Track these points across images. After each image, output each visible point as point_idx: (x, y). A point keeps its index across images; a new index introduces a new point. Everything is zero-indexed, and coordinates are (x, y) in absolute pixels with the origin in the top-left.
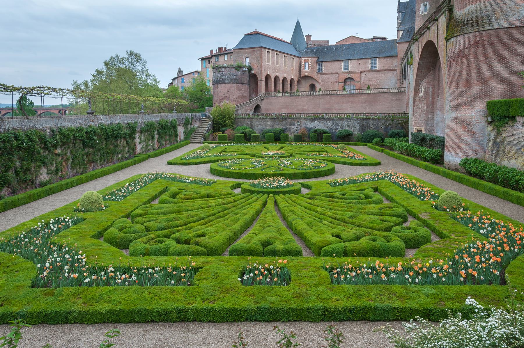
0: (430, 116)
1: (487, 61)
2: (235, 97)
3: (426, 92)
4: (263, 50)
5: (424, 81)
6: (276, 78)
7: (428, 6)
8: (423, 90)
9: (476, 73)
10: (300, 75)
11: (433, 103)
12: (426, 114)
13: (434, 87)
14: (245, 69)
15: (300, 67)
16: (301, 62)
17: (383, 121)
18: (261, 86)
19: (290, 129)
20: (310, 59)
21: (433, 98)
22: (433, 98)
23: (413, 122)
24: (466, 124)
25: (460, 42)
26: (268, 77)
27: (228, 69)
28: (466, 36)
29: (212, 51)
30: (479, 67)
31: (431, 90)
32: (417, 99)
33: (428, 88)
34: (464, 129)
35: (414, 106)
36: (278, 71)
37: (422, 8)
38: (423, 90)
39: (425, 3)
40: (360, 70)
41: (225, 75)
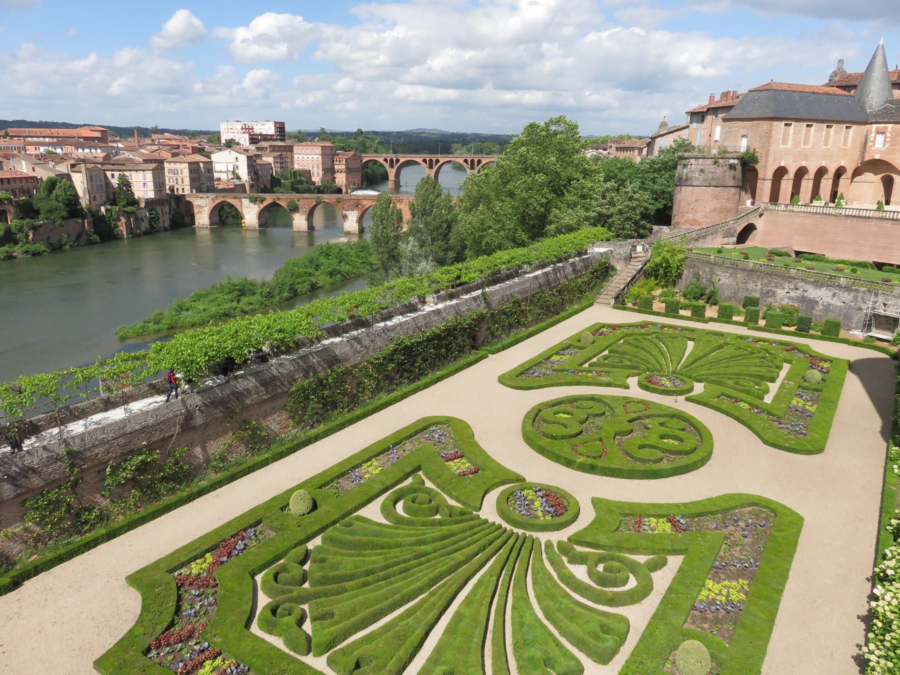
2: (708, 210)
4: (775, 123)
6: (801, 172)
10: (863, 157)
14: (731, 161)
15: (866, 143)
16: (868, 132)
18: (762, 189)
19: (774, 293)
20: (890, 126)
26: (781, 172)
27: (701, 160)
29: (711, 98)
36: (806, 157)
41: (694, 172)
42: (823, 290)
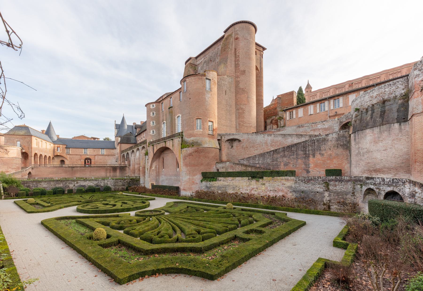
3: (156, 167)
7: (155, 132)
11: (159, 172)
21: (159, 170)
22: (159, 170)
25: (189, 150)
31: (158, 167)
37: (151, 132)
40: (95, 154)
42: (87, 182)
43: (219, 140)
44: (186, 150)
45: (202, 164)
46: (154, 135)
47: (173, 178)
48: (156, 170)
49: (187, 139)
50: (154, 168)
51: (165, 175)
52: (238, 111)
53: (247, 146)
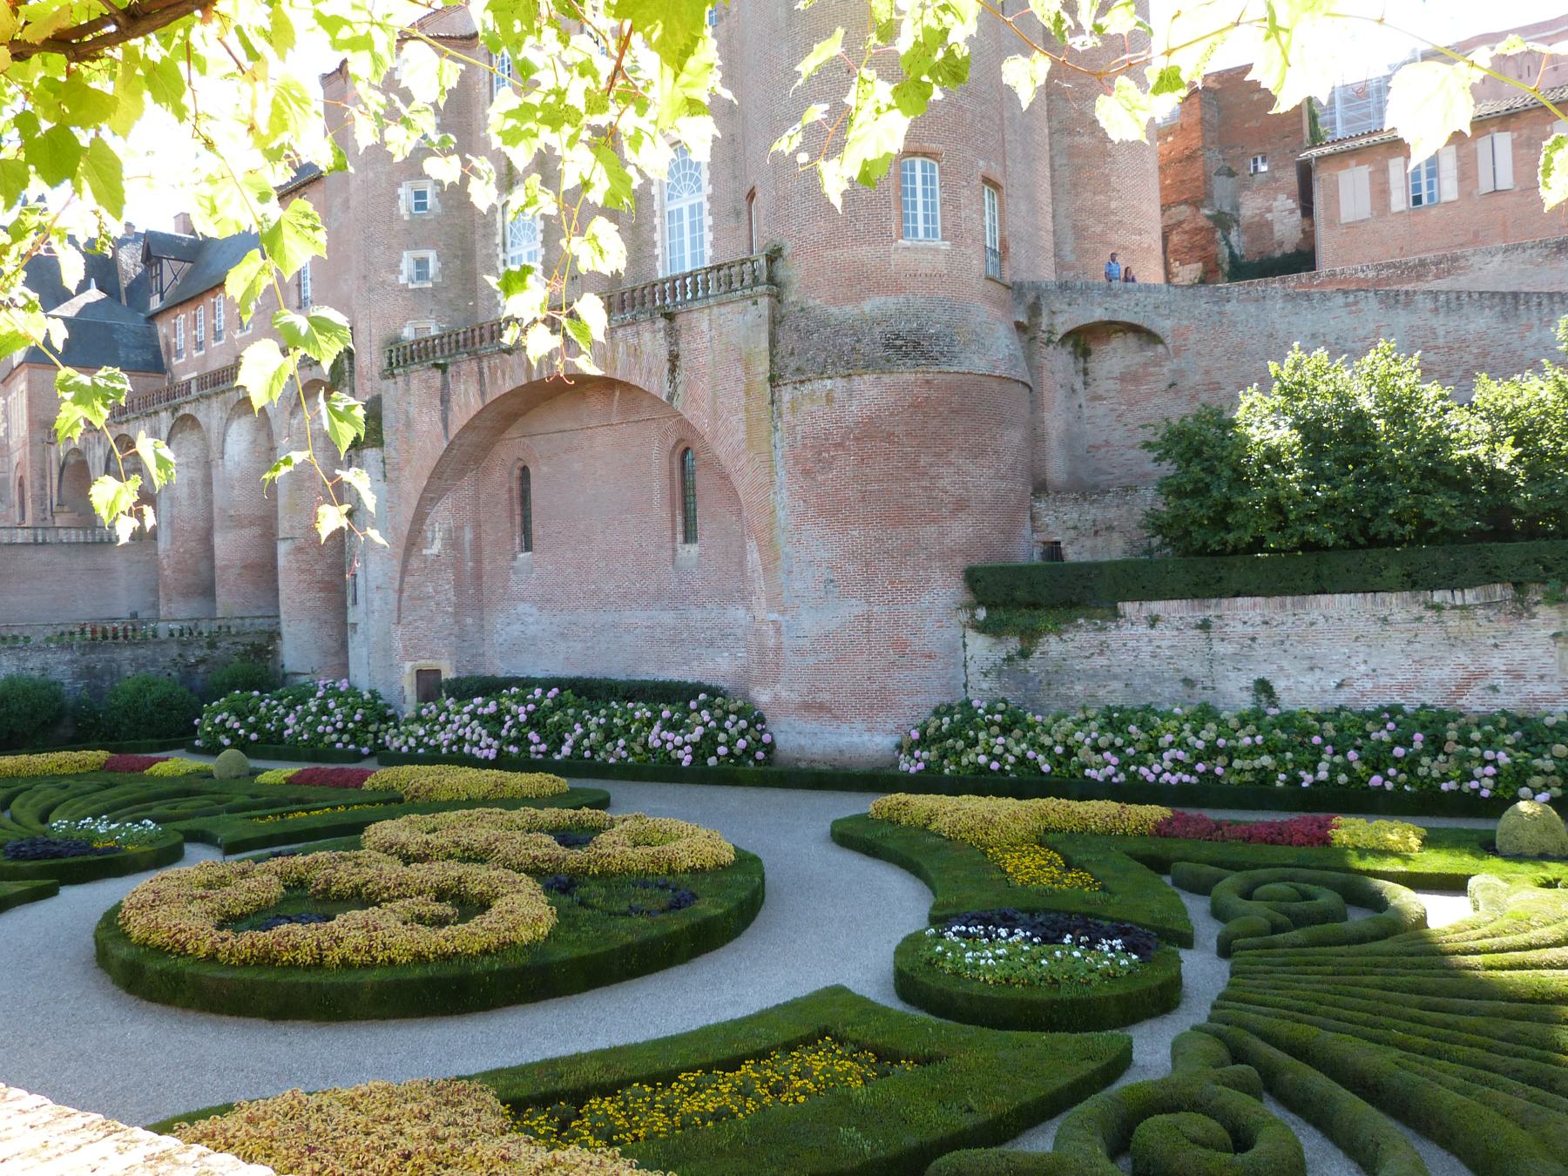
0: (469, 621)
1: (952, 457)
3: (453, 542)
5: (440, 506)
8: (439, 535)
9: (925, 489)
11: (478, 575)
12: (456, 614)
13: (477, 526)
17: (174, 651)
21: (478, 561)
23: (398, 645)
24: (904, 633)
28: (886, 379)
30: (933, 471)
31: (468, 535)
32: (415, 563)
33: (460, 528)
34: (901, 647)
35: (401, 591)
38: (439, 535)
39: (421, 253)
43: (1019, 326)
44: (830, 399)
45: (960, 506)
46: (434, 293)
47: (637, 617)
48: (457, 565)
49: (833, 310)
50: (435, 548)
51: (544, 602)
52: (1067, 140)
53: (1217, 376)
